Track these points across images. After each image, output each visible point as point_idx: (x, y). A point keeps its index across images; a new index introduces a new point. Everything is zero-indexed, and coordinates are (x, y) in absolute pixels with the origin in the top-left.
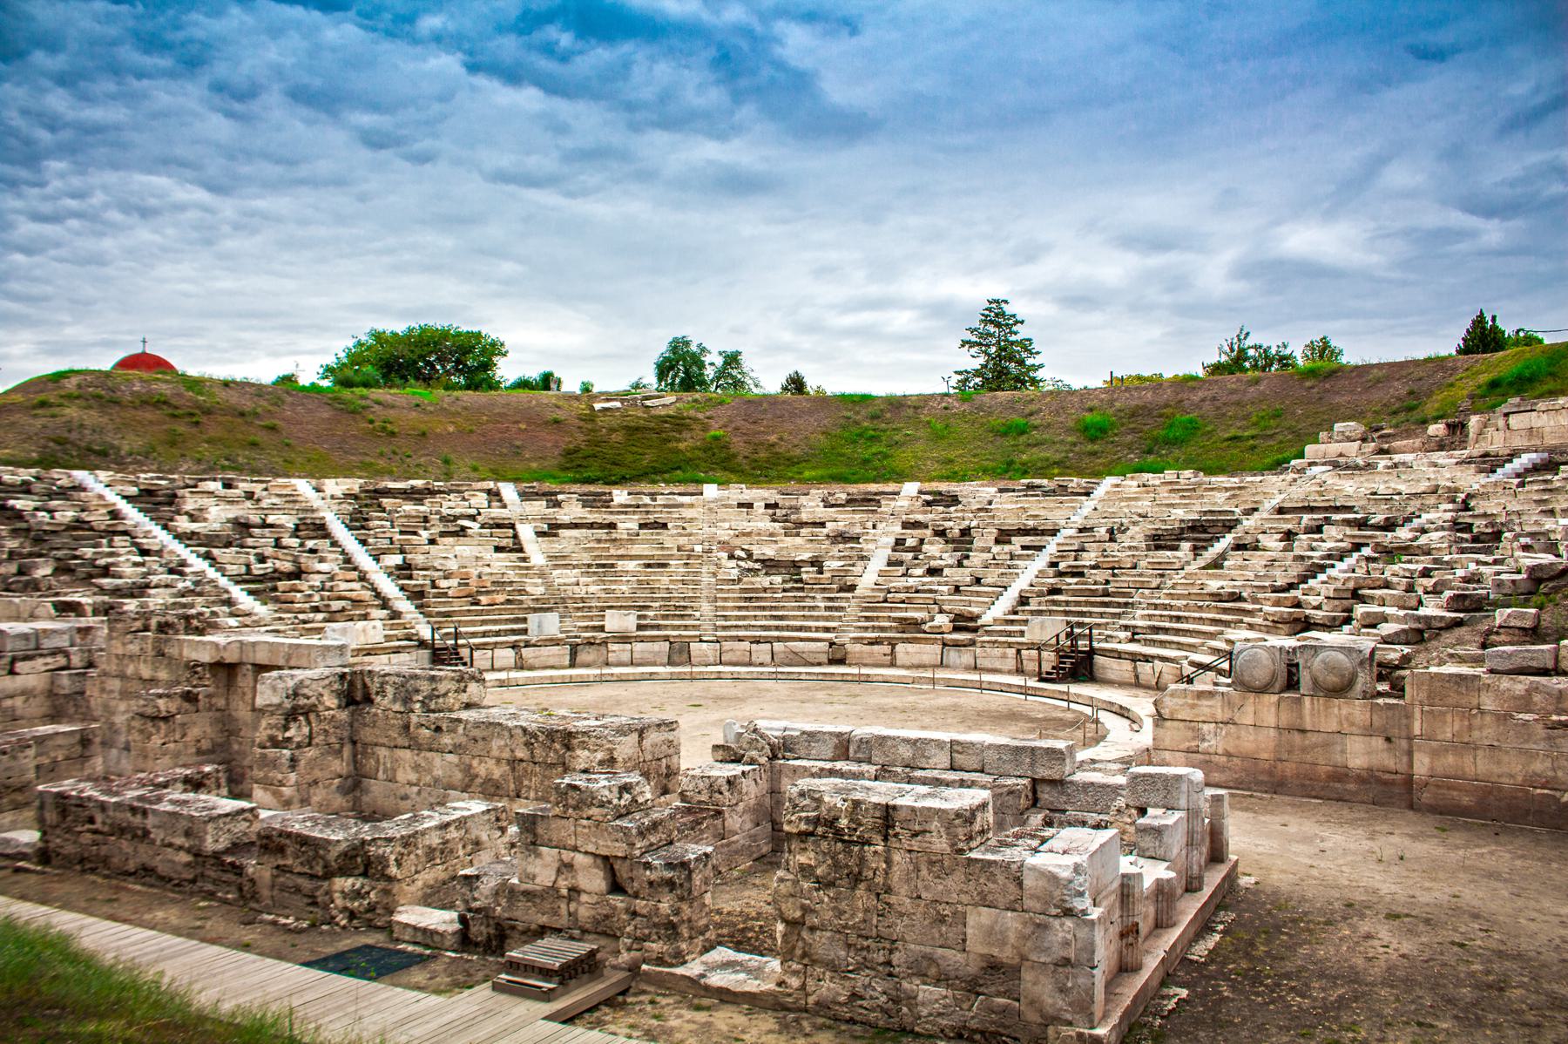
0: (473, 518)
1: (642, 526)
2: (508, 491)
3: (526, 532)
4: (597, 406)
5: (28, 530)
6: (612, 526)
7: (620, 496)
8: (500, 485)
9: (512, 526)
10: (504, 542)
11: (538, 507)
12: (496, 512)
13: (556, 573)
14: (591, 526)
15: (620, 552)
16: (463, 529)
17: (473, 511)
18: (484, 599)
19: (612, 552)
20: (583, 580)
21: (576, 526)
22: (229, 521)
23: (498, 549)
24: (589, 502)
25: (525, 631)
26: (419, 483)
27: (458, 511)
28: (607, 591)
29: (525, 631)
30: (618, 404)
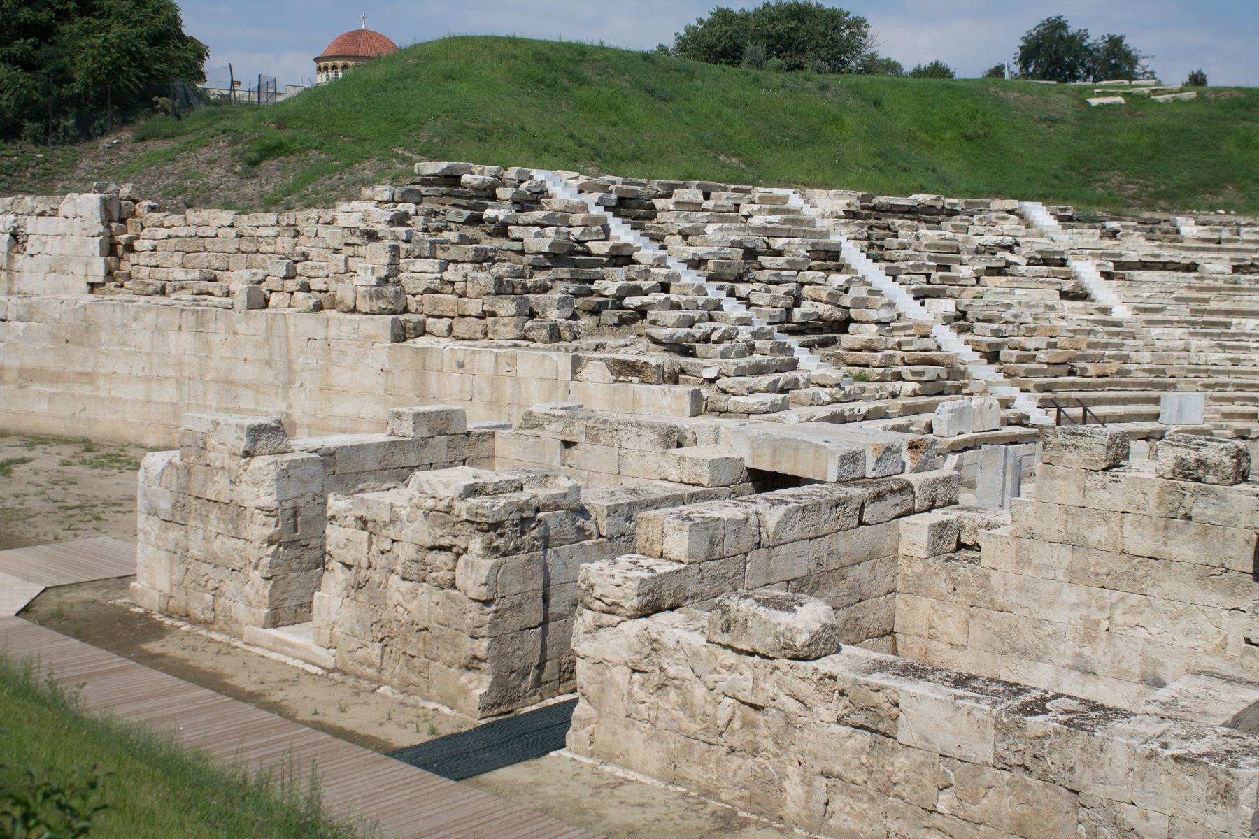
0: (1010, 248)
1: (1236, 269)
2: (1039, 213)
3: (1087, 271)
4: (1094, 102)
5: (521, 252)
6: (1191, 267)
7: (1188, 228)
8: (1026, 204)
9: (1063, 263)
10: (1068, 286)
11: (1088, 237)
12: (1042, 244)
13: (1156, 331)
14: (1164, 266)
15: (1226, 306)
16: (1009, 264)
17: (1008, 240)
18: (1092, 369)
19: (1213, 305)
20: (1195, 343)
21: (1144, 266)
22: (734, 244)
23: (1064, 295)
24: (1150, 230)
25: (1156, 417)
26: (925, 198)
27: (990, 239)
28: (1235, 362)
29: (1156, 417)
30: (1120, 100)
